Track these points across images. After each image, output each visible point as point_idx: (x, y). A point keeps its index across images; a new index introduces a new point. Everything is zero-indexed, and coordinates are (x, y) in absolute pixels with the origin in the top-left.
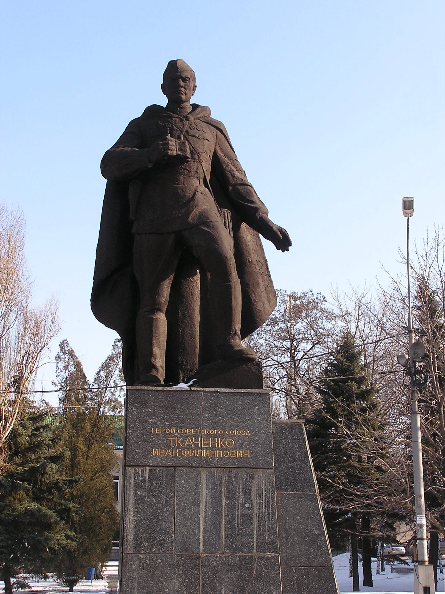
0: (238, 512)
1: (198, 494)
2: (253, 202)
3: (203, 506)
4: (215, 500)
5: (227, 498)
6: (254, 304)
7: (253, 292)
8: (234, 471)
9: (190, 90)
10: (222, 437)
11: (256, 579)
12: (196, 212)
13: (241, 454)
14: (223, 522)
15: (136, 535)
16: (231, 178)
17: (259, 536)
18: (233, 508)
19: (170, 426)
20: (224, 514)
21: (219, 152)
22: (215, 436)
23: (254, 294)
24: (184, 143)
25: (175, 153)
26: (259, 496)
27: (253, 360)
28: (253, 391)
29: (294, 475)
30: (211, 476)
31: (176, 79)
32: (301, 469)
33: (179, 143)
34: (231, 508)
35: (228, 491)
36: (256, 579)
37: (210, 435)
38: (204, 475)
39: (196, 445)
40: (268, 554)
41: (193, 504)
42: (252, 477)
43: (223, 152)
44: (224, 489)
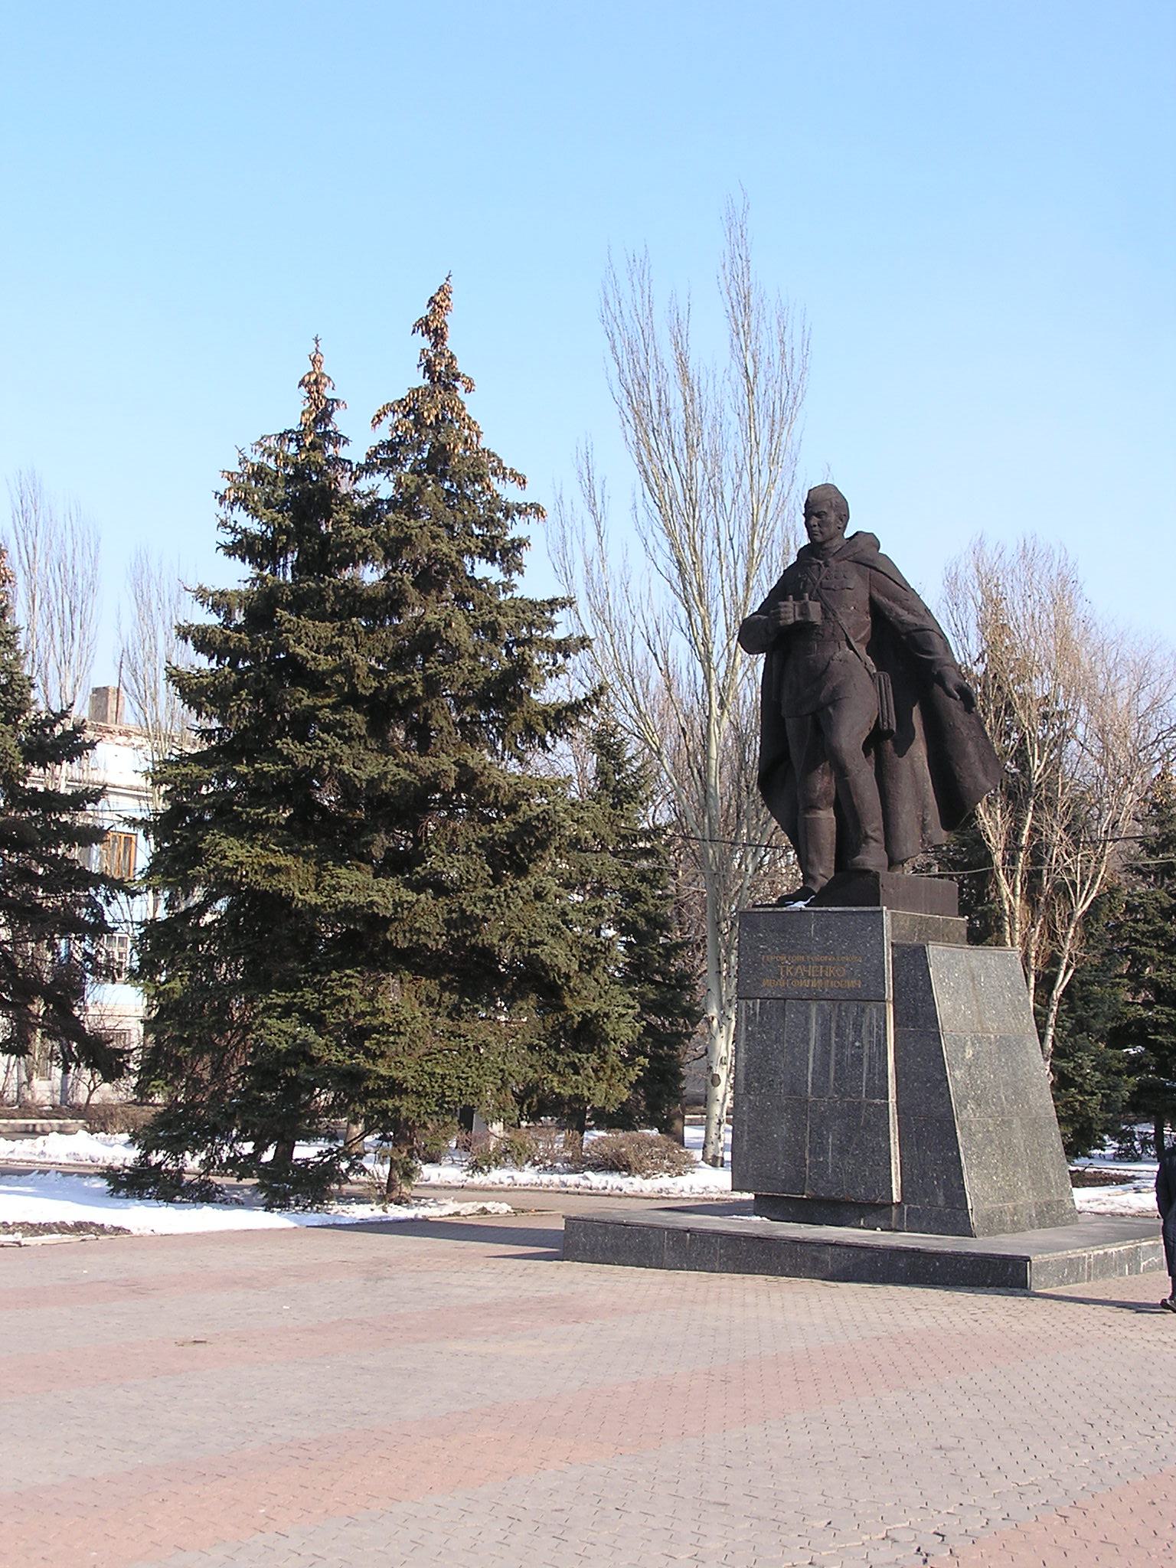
0: (848, 1052)
1: (808, 1030)
2: (930, 653)
3: (812, 1043)
4: (825, 1037)
5: (837, 1035)
8: (845, 1004)
9: (828, 525)
10: (833, 964)
11: (864, 1128)
12: (829, 686)
13: (852, 983)
14: (832, 1063)
15: (747, 1074)
16: (899, 626)
17: (868, 1079)
18: (843, 1047)
19: (782, 952)
20: (833, 1053)
21: (876, 595)
22: (826, 963)
24: (806, 604)
25: (790, 621)
26: (871, 1033)
27: (868, 871)
28: (866, 909)
29: (915, 1009)
30: (821, 1009)
31: (824, 509)
32: (924, 1001)
33: (801, 608)
34: (841, 1046)
35: (838, 1027)
36: (864, 1128)
37: (819, 963)
38: (814, 1008)
39: (806, 974)
40: (877, 1101)
41: (802, 1040)
42: (863, 1011)
43: (884, 595)
44: (833, 1025)
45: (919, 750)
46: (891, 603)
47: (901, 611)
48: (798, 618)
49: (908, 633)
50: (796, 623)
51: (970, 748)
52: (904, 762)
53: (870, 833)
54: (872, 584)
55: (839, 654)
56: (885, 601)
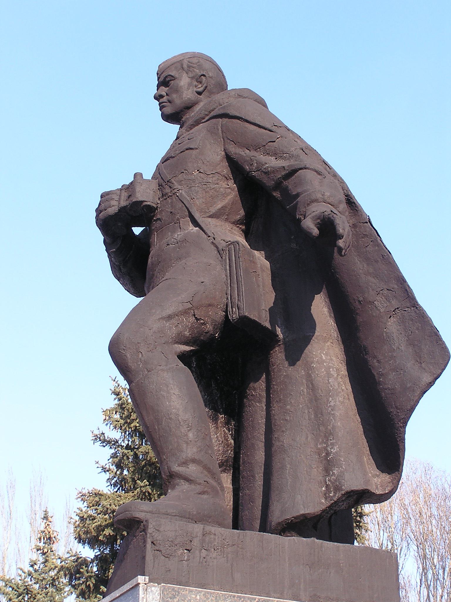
6: (380, 381)
7: (375, 357)
9: (177, 90)
21: (233, 150)
23: (378, 361)
45: (326, 354)
46: (253, 153)
47: (262, 158)
48: (123, 203)
49: (278, 185)
50: (122, 210)
51: (392, 326)
52: (298, 372)
53: (176, 468)
54: (228, 137)
55: (179, 235)
56: (245, 153)
